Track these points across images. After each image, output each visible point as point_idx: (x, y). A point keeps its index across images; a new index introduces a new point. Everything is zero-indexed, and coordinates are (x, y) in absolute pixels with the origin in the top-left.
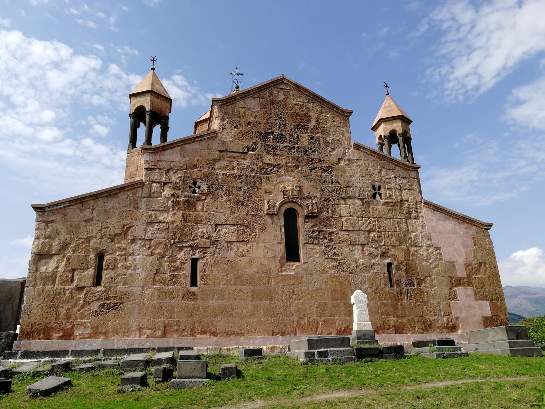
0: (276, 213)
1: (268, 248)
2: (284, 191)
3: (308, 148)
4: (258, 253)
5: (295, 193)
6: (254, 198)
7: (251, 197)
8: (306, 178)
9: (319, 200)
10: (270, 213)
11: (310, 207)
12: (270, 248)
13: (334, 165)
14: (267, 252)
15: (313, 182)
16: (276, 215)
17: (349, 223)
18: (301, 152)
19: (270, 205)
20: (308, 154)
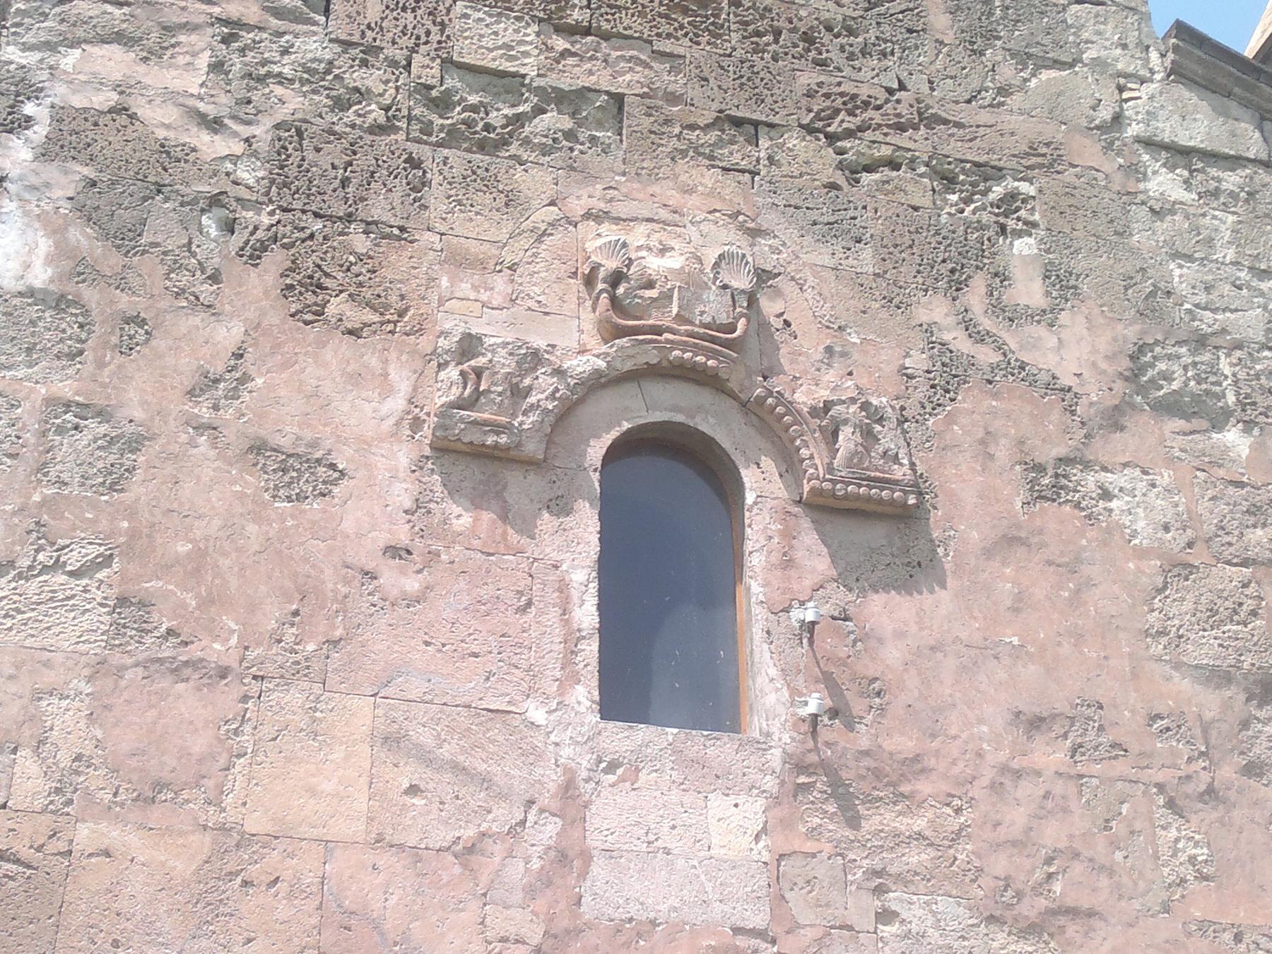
0: (533, 448)
1: (426, 758)
2: (617, 278)
3: (829, 29)
4: (313, 792)
5: (714, 307)
6: (335, 307)
7: (310, 298)
8: (814, 215)
9: (918, 396)
10: (474, 436)
11: (845, 434)
12: (445, 752)
13: (1034, 160)
14: (413, 790)
15: (867, 253)
16: (530, 464)
17: (1188, 606)
18: (769, 38)
19: (478, 373)
20: (823, 64)
